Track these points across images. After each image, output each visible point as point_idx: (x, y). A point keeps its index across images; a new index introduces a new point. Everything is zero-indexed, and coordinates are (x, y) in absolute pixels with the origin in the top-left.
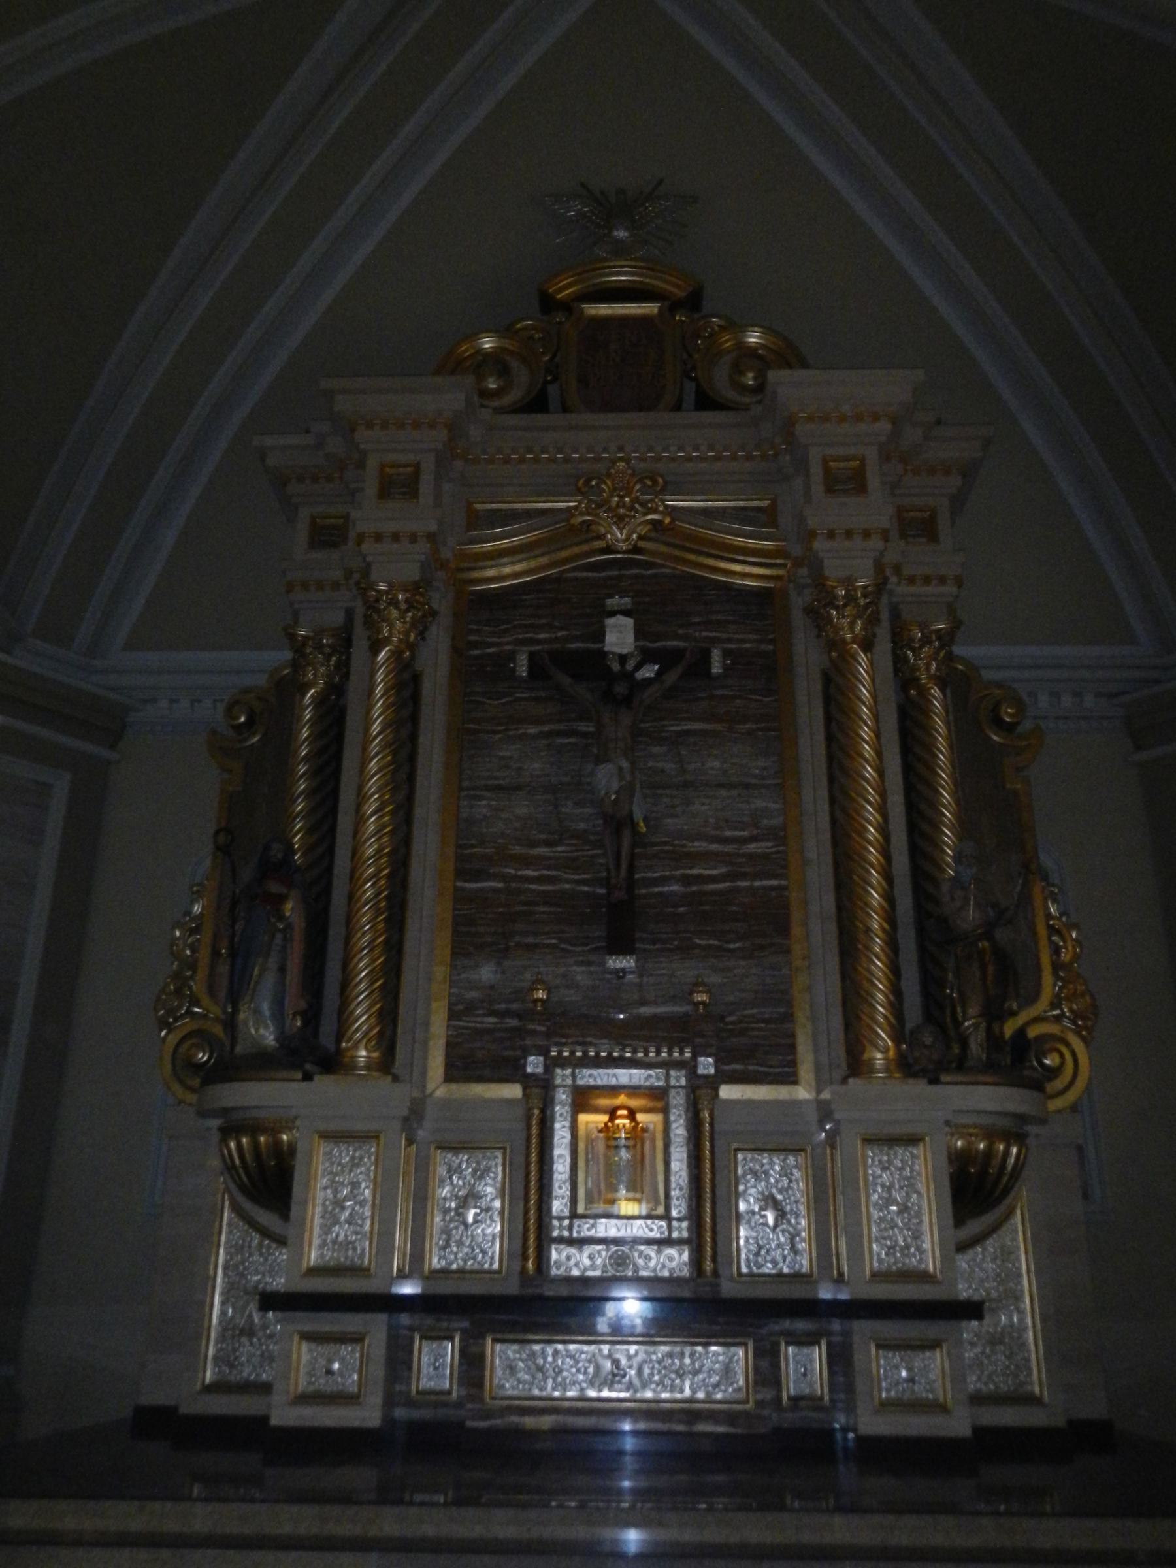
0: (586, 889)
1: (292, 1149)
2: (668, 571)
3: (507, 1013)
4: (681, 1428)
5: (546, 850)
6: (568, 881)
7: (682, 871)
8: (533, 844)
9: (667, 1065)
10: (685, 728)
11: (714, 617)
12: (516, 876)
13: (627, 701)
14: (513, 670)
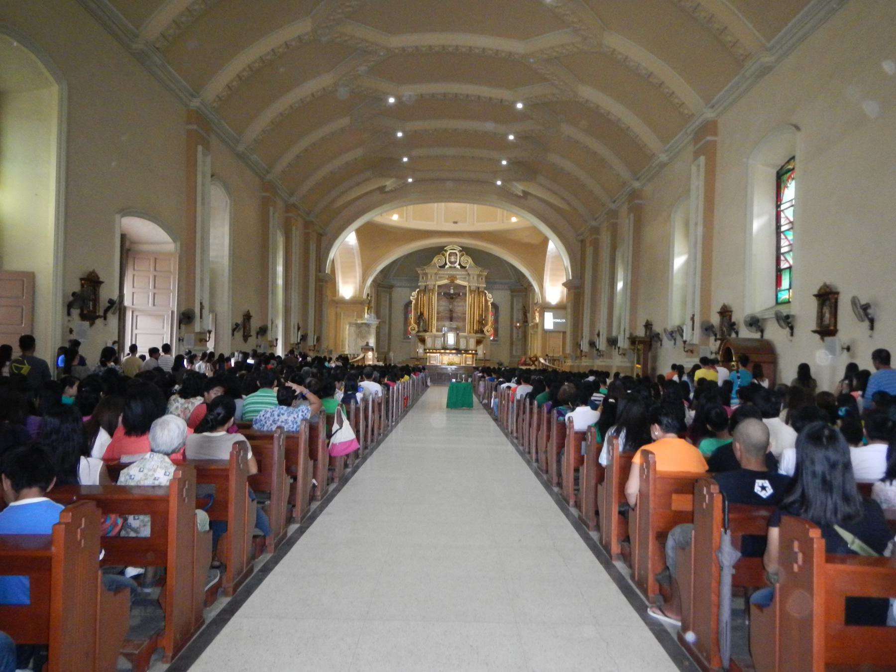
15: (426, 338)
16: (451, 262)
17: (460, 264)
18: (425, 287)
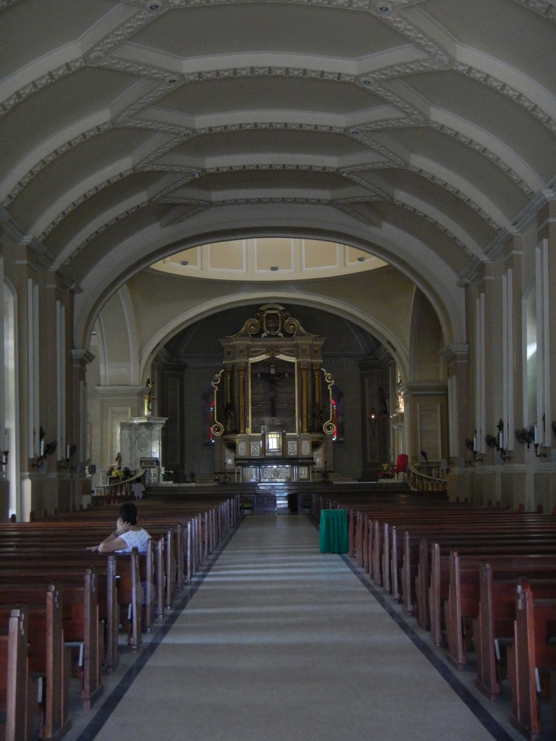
15: (237, 442)
16: (268, 328)
17: (283, 331)
18: (233, 366)
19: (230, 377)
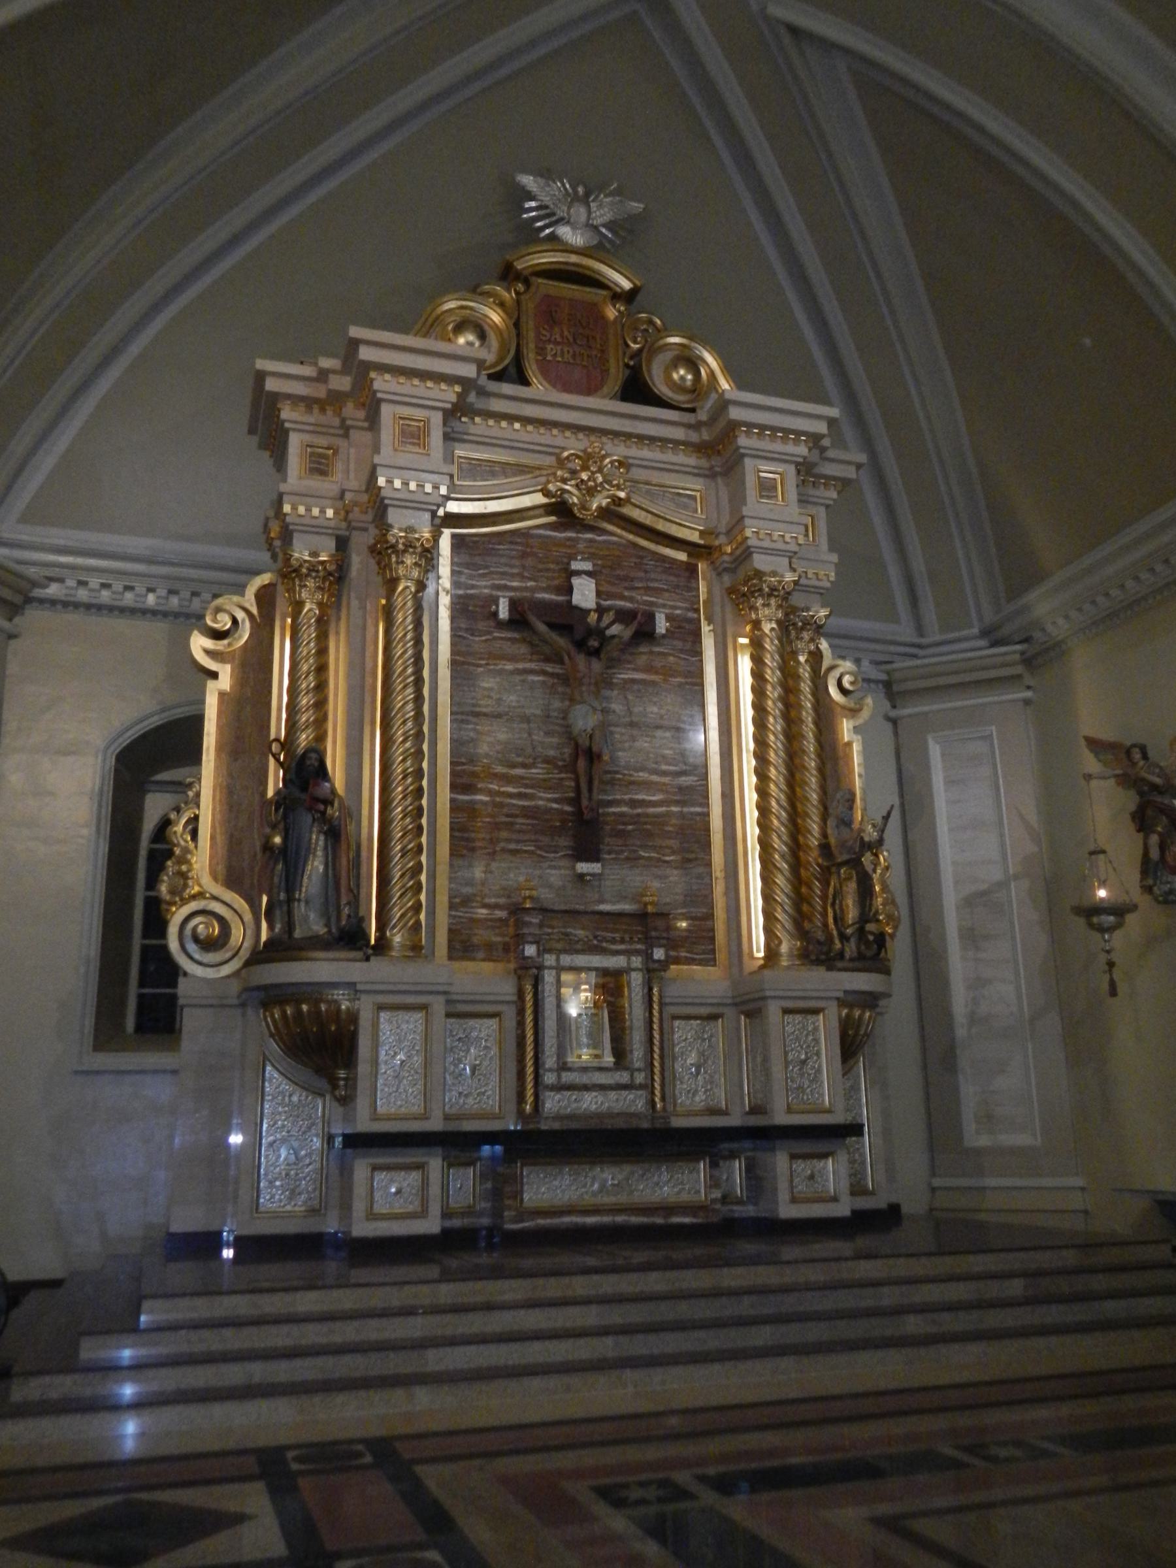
0: (555, 806)
1: (353, 1017)
2: (615, 539)
3: (496, 906)
4: (659, 1220)
5: (524, 771)
6: (541, 798)
7: (630, 796)
8: (513, 766)
9: (628, 953)
10: (631, 676)
11: (651, 585)
12: (499, 791)
13: (596, 653)
14: (496, 614)
19: (320, 605)
